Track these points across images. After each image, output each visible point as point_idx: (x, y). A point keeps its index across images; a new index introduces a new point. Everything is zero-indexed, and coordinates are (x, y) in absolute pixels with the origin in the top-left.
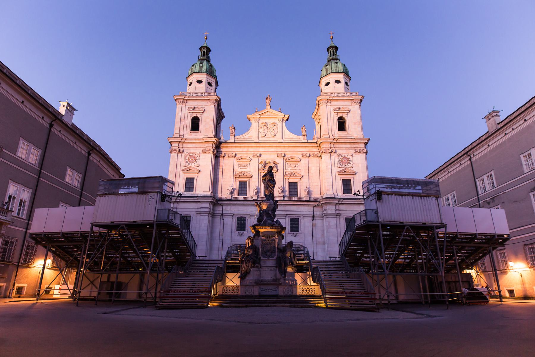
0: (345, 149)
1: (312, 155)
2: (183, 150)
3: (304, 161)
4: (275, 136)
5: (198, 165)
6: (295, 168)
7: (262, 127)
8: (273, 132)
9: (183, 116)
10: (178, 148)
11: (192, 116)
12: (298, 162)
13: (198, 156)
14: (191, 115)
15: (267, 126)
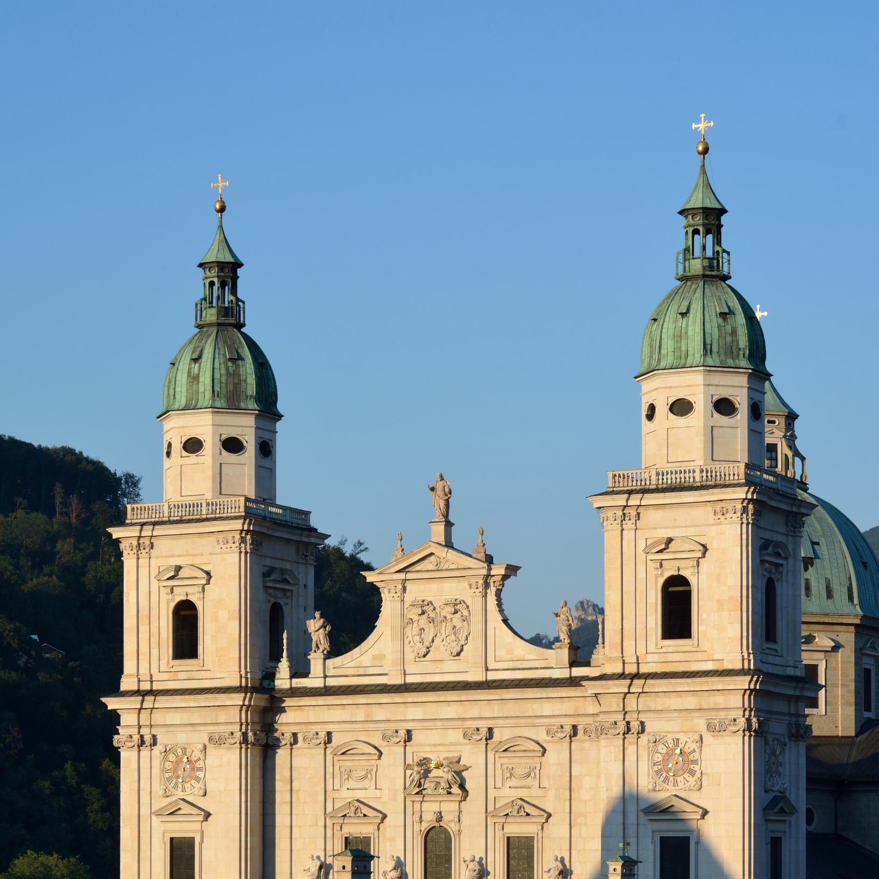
0: (676, 714)
1: (580, 732)
2: (154, 737)
3: (557, 754)
4: (458, 654)
5: (202, 792)
6: (528, 782)
7: (415, 618)
8: (453, 637)
9: (143, 603)
10: (136, 730)
11: (173, 600)
12: (537, 760)
13: (202, 758)
14: (171, 596)
15: (432, 615)
